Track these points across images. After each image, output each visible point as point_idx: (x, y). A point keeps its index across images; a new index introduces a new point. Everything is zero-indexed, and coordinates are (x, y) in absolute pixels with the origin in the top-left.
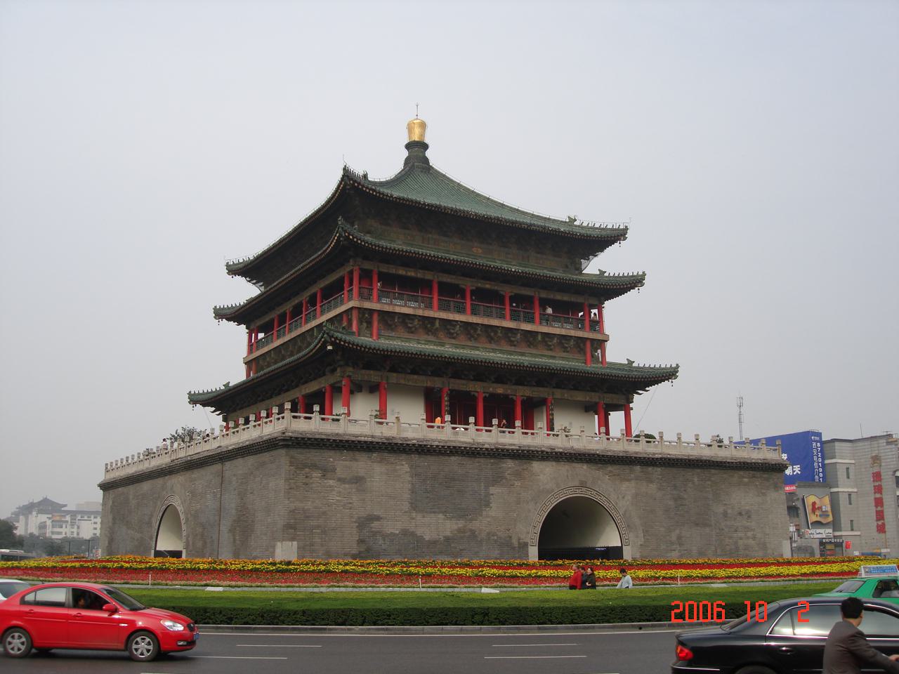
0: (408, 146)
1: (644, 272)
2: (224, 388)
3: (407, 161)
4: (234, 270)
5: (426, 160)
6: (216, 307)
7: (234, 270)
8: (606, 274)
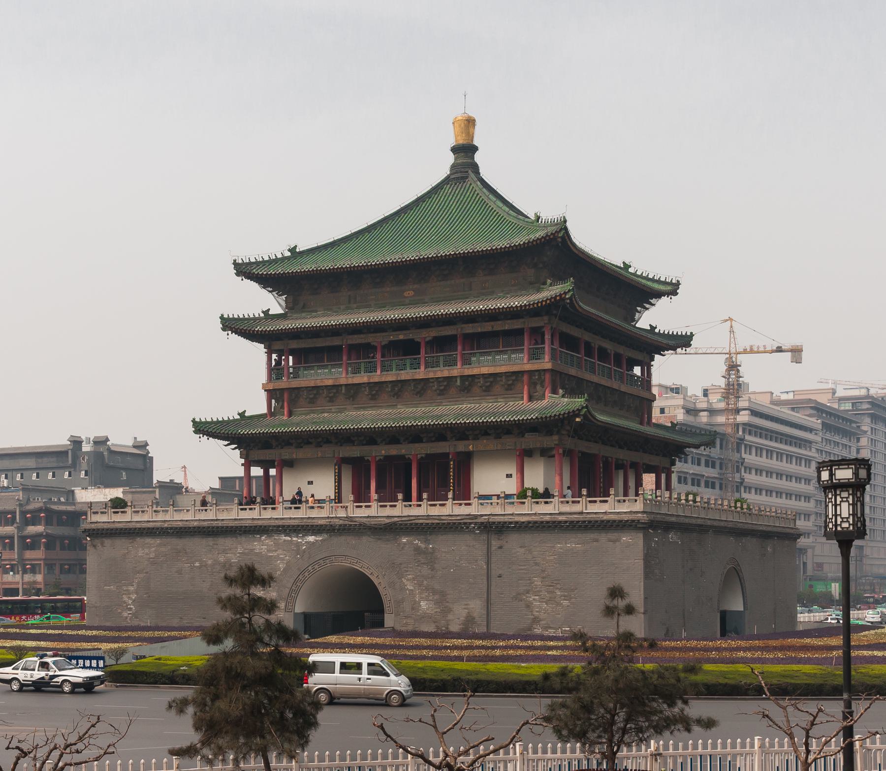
1: (691, 333)
4: (244, 270)
6: (222, 315)
7: (244, 270)
8: (657, 331)
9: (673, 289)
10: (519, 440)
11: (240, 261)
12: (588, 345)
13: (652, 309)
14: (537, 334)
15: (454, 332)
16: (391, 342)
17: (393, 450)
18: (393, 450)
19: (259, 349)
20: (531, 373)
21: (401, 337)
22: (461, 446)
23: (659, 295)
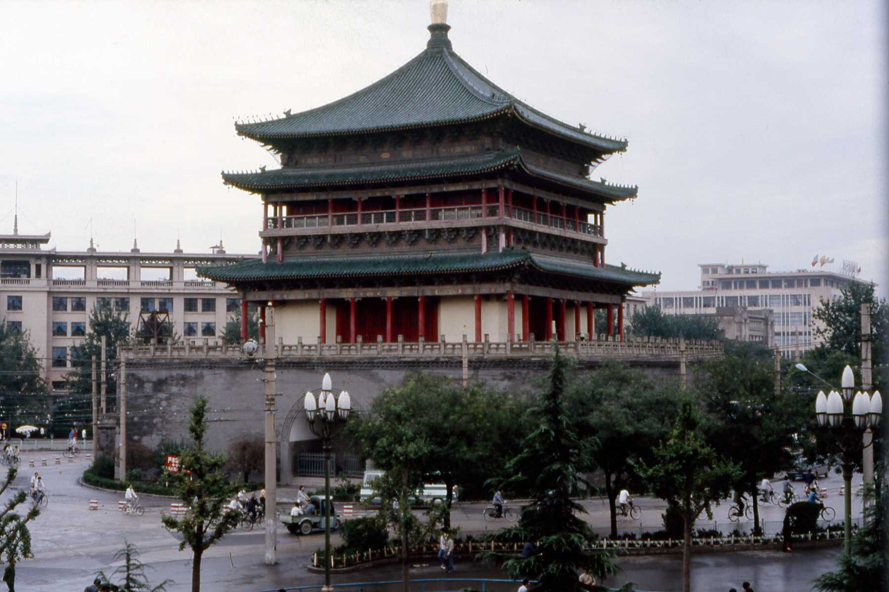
0: (433, 28)
3: (430, 43)
4: (245, 130)
5: (448, 44)
7: (245, 130)
9: (621, 146)
10: (480, 284)
12: (540, 200)
13: (604, 163)
14: (493, 195)
15: (424, 192)
16: (370, 198)
17: (370, 293)
18: (370, 293)
19: (258, 198)
21: (378, 194)
22: (430, 291)
23: (610, 151)
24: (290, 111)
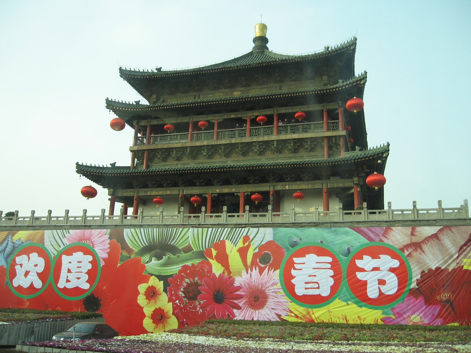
2: (110, 166)
11: (124, 69)
15: (272, 113)
17: (226, 190)
20: (329, 138)
22: (279, 187)
24: (161, 68)
